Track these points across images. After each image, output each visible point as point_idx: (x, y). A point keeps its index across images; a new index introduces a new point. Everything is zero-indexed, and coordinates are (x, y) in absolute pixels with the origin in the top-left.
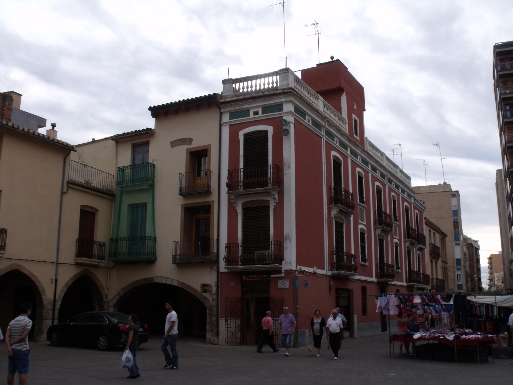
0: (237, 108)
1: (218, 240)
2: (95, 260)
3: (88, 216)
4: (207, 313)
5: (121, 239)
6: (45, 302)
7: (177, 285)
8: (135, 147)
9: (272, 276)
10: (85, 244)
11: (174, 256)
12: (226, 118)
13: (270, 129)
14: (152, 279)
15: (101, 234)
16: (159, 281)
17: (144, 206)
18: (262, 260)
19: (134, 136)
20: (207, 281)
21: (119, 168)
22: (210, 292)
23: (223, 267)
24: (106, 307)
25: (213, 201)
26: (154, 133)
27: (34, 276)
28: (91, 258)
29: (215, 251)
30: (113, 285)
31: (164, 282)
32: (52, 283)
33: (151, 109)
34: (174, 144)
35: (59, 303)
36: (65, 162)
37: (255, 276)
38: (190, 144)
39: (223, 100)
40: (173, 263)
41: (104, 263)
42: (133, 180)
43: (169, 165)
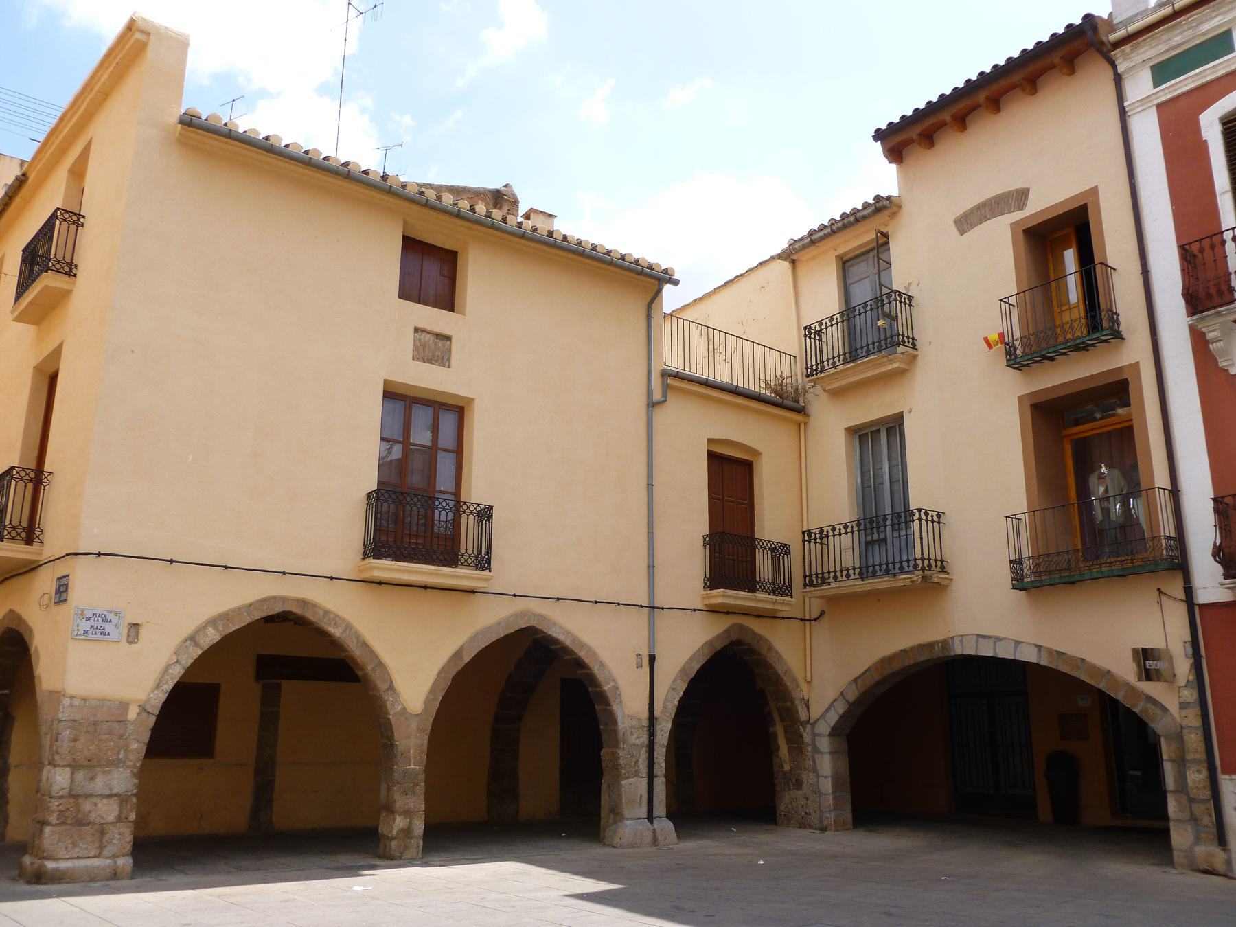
0: (1178, 39)
1: (1174, 492)
2: (765, 596)
4: (1165, 757)
5: (834, 529)
6: (623, 724)
11: (1016, 563)
14: (945, 644)
15: (775, 520)
16: (970, 651)
19: (840, 229)
20: (1153, 640)
21: (808, 328)
22: (1171, 678)
23: (1210, 582)
24: (807, 738)
25: (1136, 366)
26: (900, 207)
27: (583, 645)
28: (754, 590)
30: (824, 670)
31: (989, 653)
32: (639, 666)
33: (879, 135)
34: (965, 223)
35: (664, 728)
36: (649, 317)
38: (1021, 207)
39: (1121, 33)
40: (1014, 587)
41: (790, 604)
43: (963, 284)
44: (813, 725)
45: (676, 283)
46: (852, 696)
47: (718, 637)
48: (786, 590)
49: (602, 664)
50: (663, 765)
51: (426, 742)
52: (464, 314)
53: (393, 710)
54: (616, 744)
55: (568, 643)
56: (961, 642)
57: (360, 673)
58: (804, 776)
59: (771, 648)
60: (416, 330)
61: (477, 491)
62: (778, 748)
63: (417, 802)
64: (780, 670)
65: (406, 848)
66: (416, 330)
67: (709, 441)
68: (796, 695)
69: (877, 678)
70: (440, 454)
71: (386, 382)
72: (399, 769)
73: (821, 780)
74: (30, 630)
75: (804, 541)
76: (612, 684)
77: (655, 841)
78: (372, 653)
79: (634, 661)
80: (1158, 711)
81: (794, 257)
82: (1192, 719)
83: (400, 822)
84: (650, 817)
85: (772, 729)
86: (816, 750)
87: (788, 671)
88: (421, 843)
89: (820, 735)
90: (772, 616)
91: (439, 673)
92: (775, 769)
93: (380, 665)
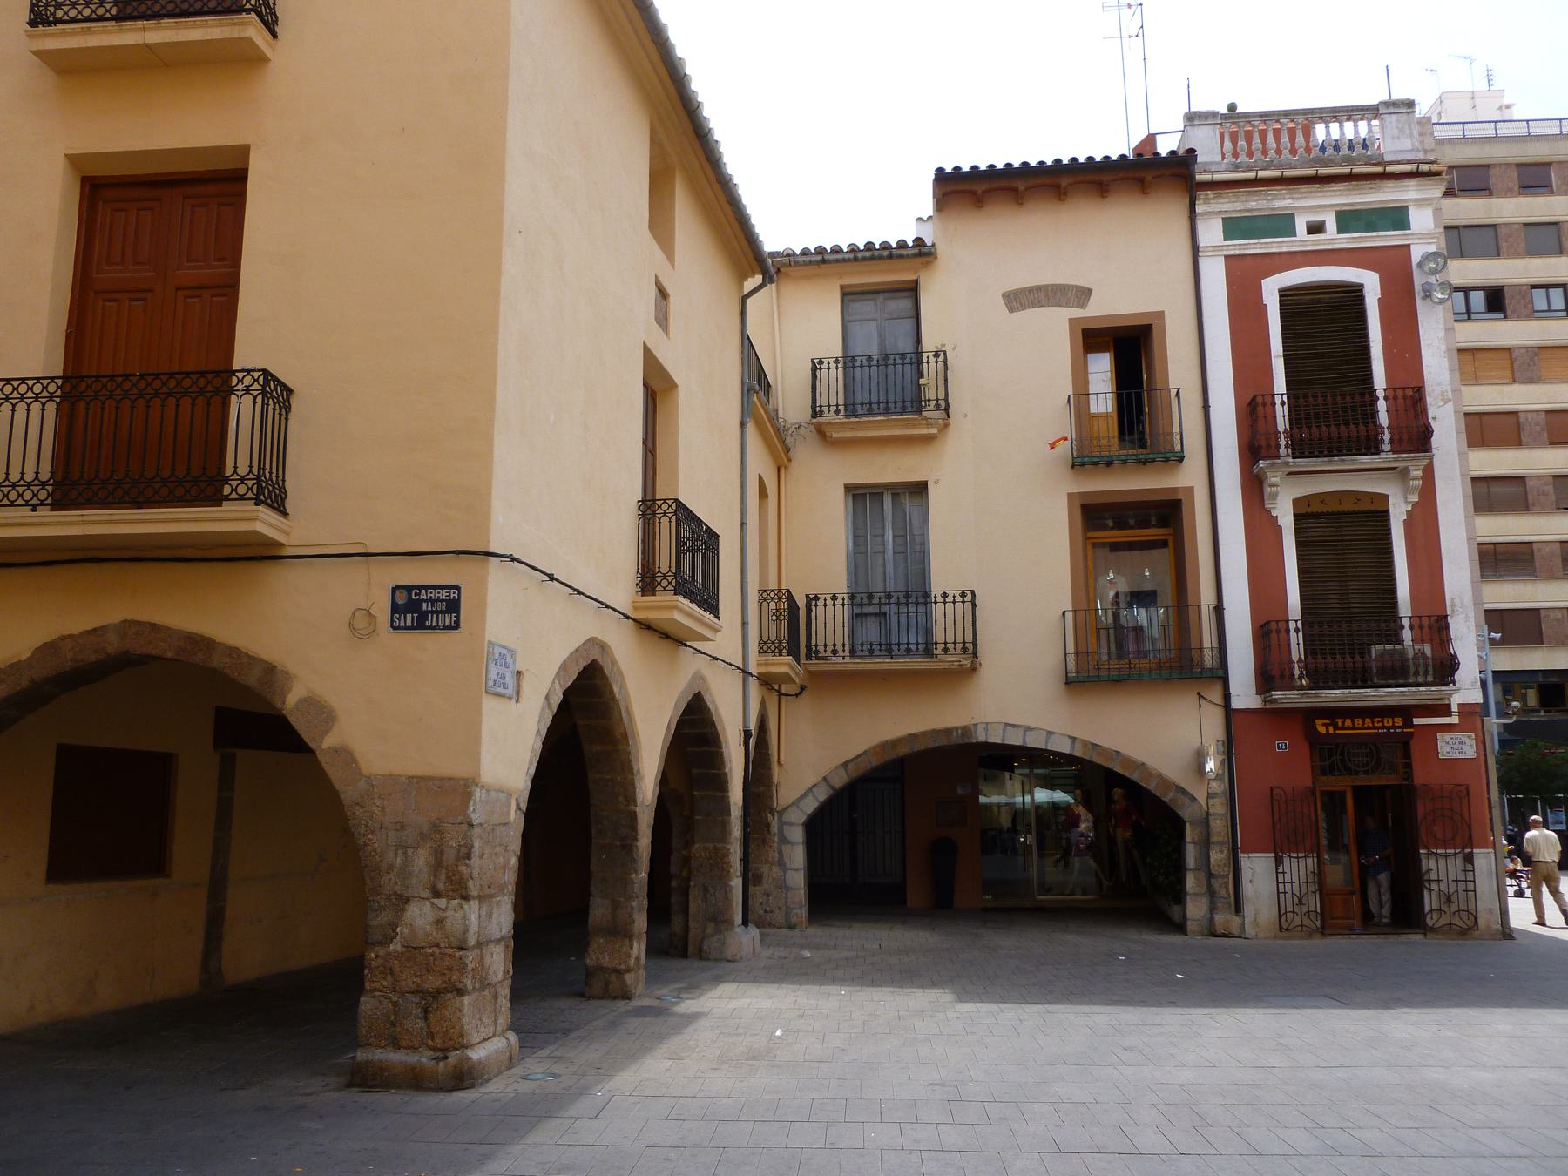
0: (1253, 204)
1: (1219, 609)
4: (1188, 839)
7: (1067, 750)
8: (848, 295)
9: (1416, 721)
12: (1211, 233)
13: (1371, 283)
14: (966, 730)
16: (995, 739)
17: (920, 489)
18: (1397, 672)
19: (864, 259)
23: (1244, 695)
25: (1191, 489)
29: (1209, 640)
34: (1018, 300)
37: (1358, 722)
39: (1206, 177)
42: (851, 409)
44: (781, 813)
46: (840, 780)
56: (986, 729)
58: (765, 869)
69: (875, 763)
73: (789, 874)
74: (270, 669)
80: (1187, 801)
82: (1219, 808)
86: (784, 840)
89: (791, 824)
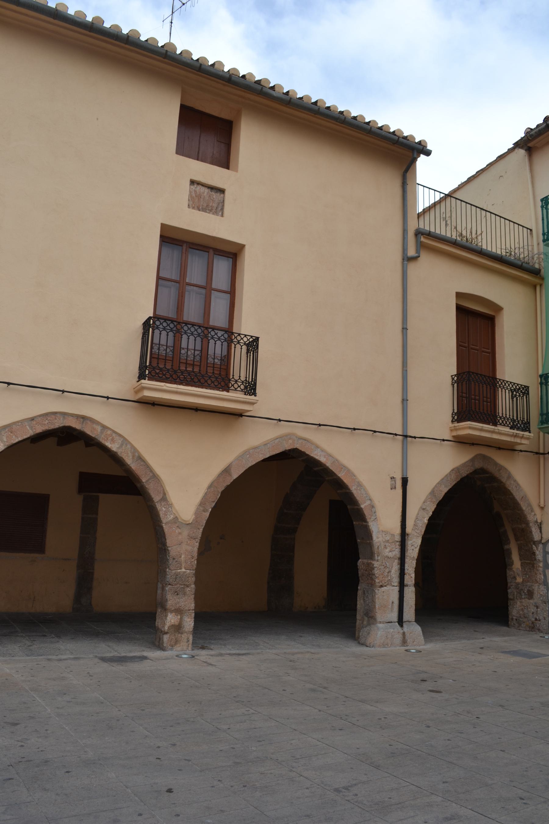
2: (507, 430)
3: (476, 323)
6: (377, 538)
10: (476, 388)
24: (539, 555)
28: (495, 424)
32: (393, 488)
41: (528, 439)
44: (545, 544)
45: (428, 153)
47: (464, 465)
48: (526, 427)
49: (360, 485)
50: (413, 575)
51: (196, 549)
52: (237, 171)
53: (166, 518)
54: (371, 556)
55: (328, 464)
57: (138, 485)
58: (536, 587)
59: (510, 476)
60: (192, 182)
61: (247, 325)
62: (512, 563)
63: (188, 602)
64: (518, 496)
65: (177, 642)
66: (192, 182)
67: (459, 295)
68: (530, 518)
70: (214, 294)
71: (164, 227)
72: (171, 573)
75: (541, 384)
76: (368, 502)
77: (404, 642)
78: (148, 466)
79: (388, 482)
81: (530, 145)
83: (171, 619)
84: (401, 621)
85: (506, 547)
87: (524, 497)
88: (191, 638)
90: (509, 449)
91: (210, 487)
92: (509, 580)
93: (155, 477)
